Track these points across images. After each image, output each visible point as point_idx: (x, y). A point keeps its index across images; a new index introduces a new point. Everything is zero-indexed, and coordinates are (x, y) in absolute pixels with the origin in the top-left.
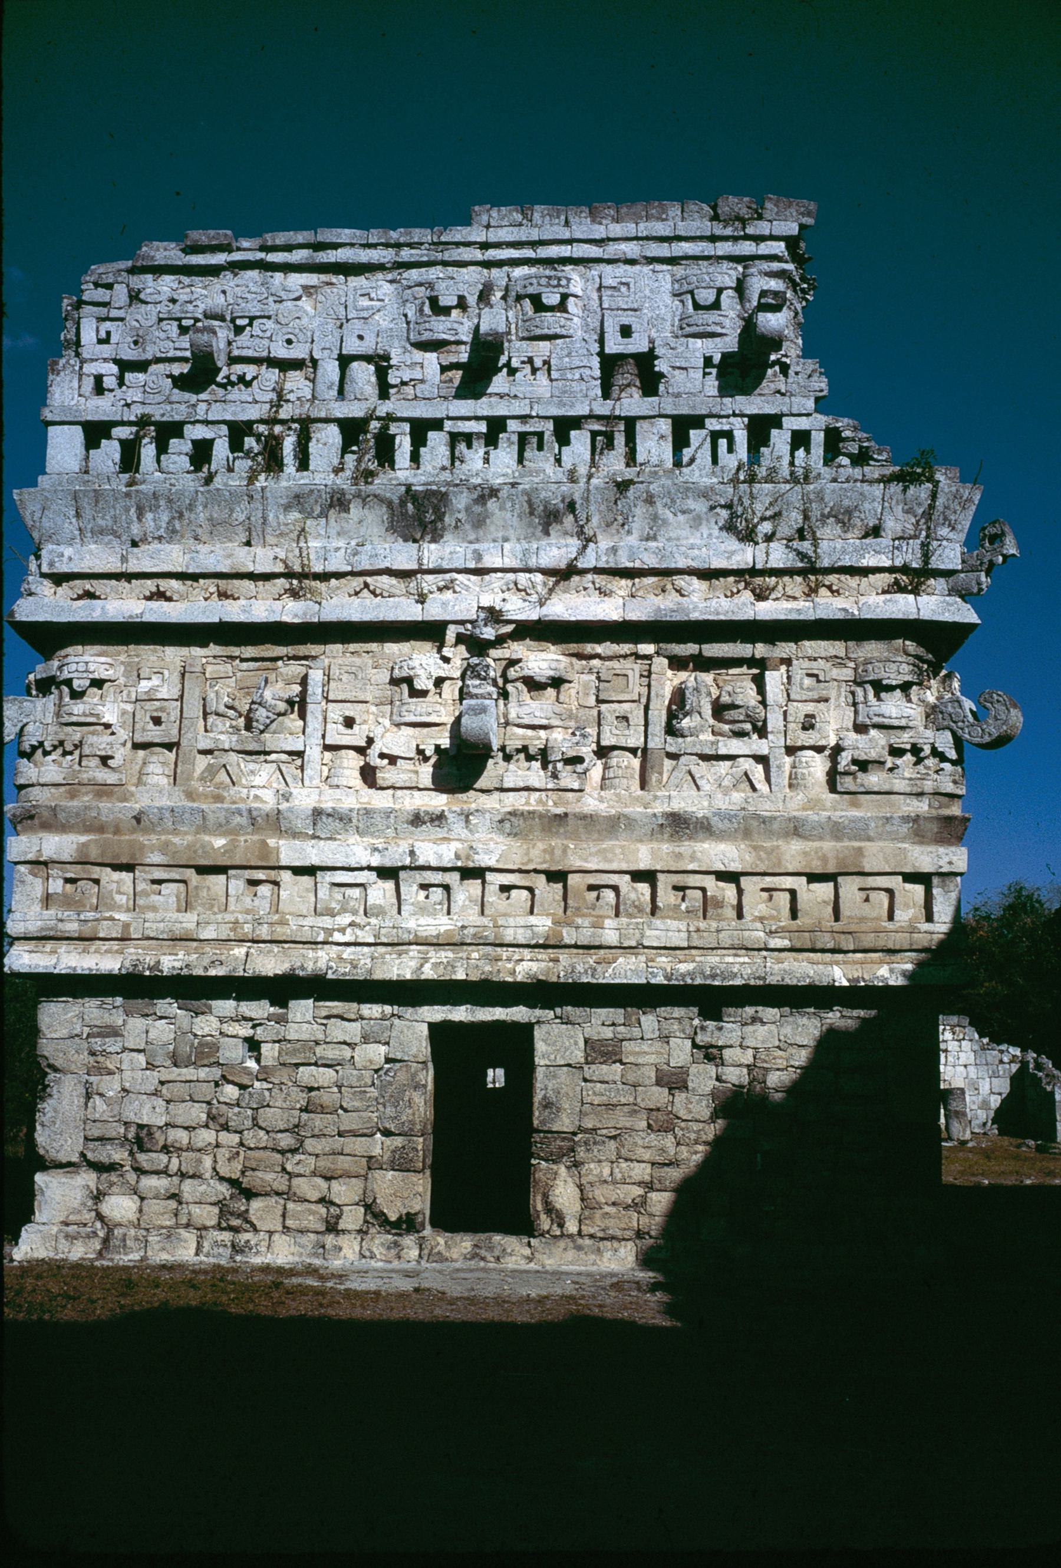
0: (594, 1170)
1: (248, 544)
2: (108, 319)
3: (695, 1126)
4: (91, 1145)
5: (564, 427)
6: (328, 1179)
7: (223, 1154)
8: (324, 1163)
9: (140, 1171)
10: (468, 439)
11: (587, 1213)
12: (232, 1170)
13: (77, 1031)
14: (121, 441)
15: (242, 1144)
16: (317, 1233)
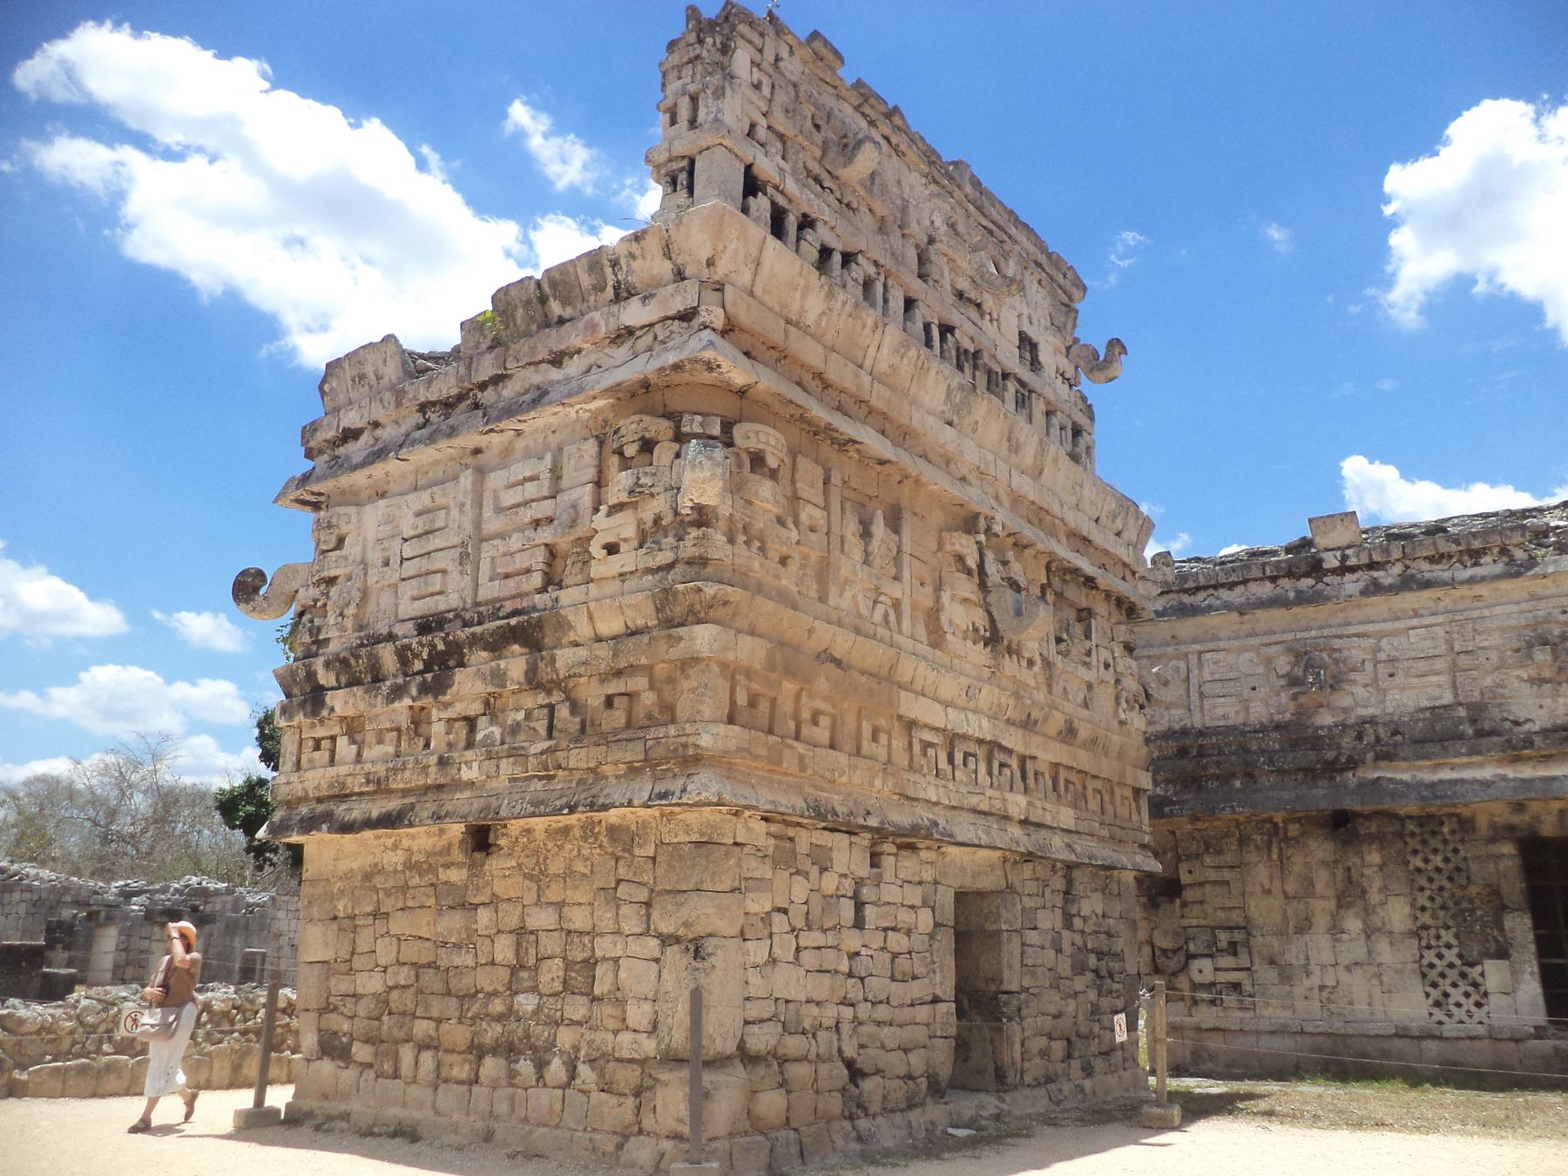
0: (1028, 1022)
1: (861, 367)
2: (758, 66)
3: (1068, 982)
4: (755, 1029)
5: (1005, 376)
6: (906, 1051)
7: (846, 1028)
8: (907, 1034)
9: (784, 1061)
10: (966, 351)
11: (1027, 1065)
12: (850, 1051)
13: (736, 884)
14: (773, 204)
15: (855, 1017)
16: (902, 1111)
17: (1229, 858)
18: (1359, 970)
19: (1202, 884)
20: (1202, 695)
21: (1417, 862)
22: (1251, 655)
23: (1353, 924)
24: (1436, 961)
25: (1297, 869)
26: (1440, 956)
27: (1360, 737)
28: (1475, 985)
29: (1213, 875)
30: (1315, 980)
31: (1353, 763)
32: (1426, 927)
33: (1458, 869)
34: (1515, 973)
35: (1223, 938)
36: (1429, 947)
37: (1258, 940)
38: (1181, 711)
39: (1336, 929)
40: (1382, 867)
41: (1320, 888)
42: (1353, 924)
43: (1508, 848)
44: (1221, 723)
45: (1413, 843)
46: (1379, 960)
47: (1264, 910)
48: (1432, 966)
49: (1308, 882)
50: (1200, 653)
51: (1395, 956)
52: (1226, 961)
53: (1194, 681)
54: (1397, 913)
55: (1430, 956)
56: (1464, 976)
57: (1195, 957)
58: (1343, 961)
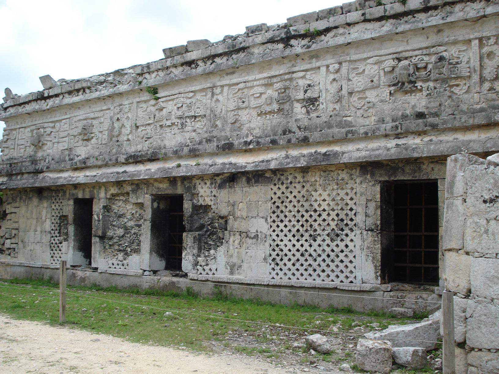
17: (17, 205)
18: (38, 244)
19: (11, 213)
20: (18, 145)
21: (53, 207)
22: (29, 129)
23: (39, 229)
24: (54, 242)
25: (30, 208)
26: (54, 240)
27: (45, 161)
28: (60, 250)
29: (13, 210)
30: (29, 248)
31: (42, 172)
32: (52, 230)
33: (61, 209)
34: (68, 247)
35: (14, 232)
36: (52, 237)
37: (20, 233)
38: (13, 150)
39: (36, 231)
40: (47, 207)
41: (34, 216)
42: (39, 229)
43: (71, 202)
44: (20, 155)
45: (53, 199)
46: (43, 241)
47: (22, 223)
48: (52, 243)
49: (32, 212)
50: (20, 128)
51: (46, 239)
52: (13, 241)
53: (17, 139)
54: (48, 225)
55: (52, 239)
56: (58, 247)
57: (7, 239)
58: (36, 242)
